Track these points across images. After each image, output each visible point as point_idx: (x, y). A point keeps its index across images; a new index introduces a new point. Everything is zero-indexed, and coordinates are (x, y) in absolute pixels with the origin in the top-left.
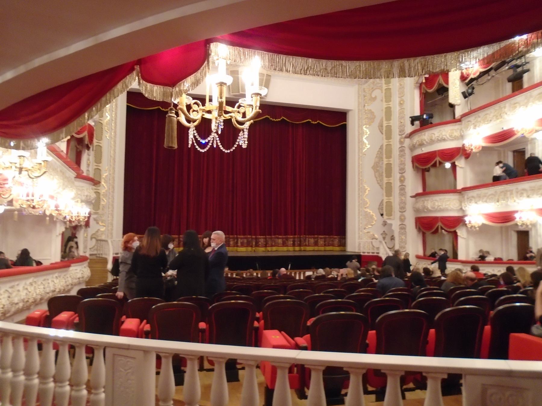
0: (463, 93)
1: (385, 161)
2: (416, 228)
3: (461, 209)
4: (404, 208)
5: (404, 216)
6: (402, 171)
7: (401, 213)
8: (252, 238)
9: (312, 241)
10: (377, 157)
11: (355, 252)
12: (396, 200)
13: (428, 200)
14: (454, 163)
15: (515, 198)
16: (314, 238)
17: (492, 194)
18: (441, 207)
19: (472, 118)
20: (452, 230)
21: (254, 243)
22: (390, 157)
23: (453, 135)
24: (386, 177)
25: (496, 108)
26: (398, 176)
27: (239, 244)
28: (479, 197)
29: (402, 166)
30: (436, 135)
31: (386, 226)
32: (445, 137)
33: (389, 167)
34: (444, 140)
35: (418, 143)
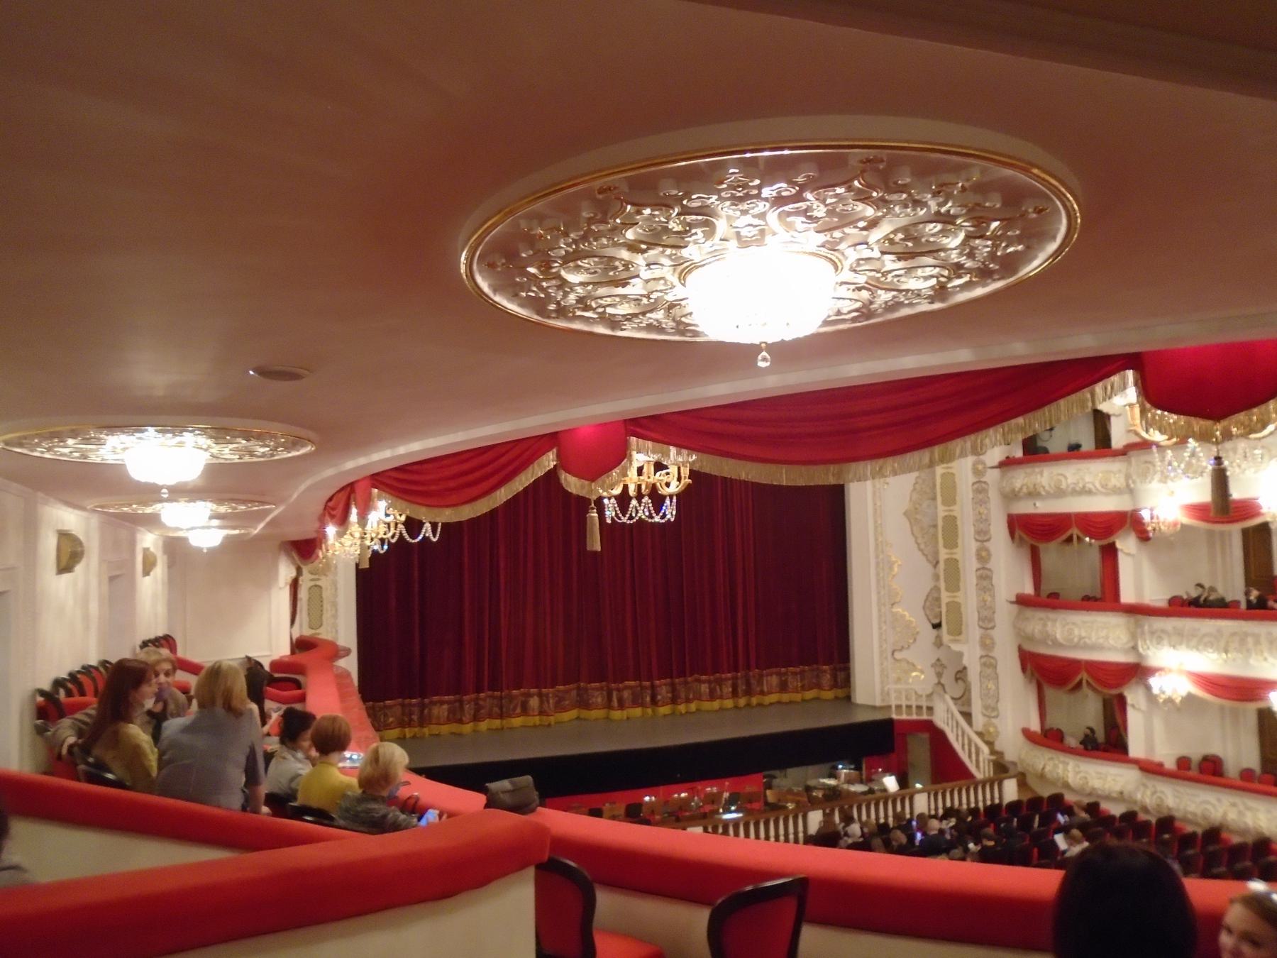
2: (1024, 669)
3: (1135, 648)
4: (991, 620)
5: (992, 639)
6: (983, 535)
8: (642, 688)
10: (914, 489)
11: (874, 708)
12: (969, 598)
13: (1055, 621)
15: (1266, 654)
16: (779, 674)
20: (1115, 692)
21: (648, 699)
22: (953, 502)
24: (945, 547)
26: (974, 546)
27: (615, 703)
30: (1070, 481)
32: (1090, 486)
33: (951, 522)
34: (1090, 492)
35: (1025, 490)
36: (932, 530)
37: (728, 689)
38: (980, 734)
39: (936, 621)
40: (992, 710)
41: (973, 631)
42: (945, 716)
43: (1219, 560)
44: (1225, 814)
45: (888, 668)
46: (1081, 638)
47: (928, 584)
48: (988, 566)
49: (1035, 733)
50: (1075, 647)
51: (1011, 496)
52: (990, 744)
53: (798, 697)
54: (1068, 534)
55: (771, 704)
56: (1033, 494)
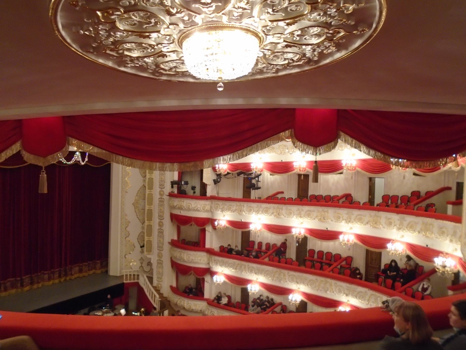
0: (214, 180)
3: (209, 263)
4: (162, 247)
5: (162, 254)
6: (161, 217)
9: (77, 269)
12: (155, 239)
14: (205, 228)
15: (247, 272)
19: (220, 203)
20: (201, 277)
21: (19, 285)
24: (147, 220)
26: (158, 221)
30: (193, 206)
33: (150, 212)
34: (199, 211)
36: (142, 211)
37: (57, 275)
39: (142, 245)
40: (160, 278)
42: (143, 282)
43: (235, 234)
45: (122, 260)
46: (192, 260)
47: (139, 230)
50: (191, 262)
51: (173, 207)
52: (158, 291)
53: (86, 274)
54: (191, 223)
55: (75, 278)
56: (180, 208)
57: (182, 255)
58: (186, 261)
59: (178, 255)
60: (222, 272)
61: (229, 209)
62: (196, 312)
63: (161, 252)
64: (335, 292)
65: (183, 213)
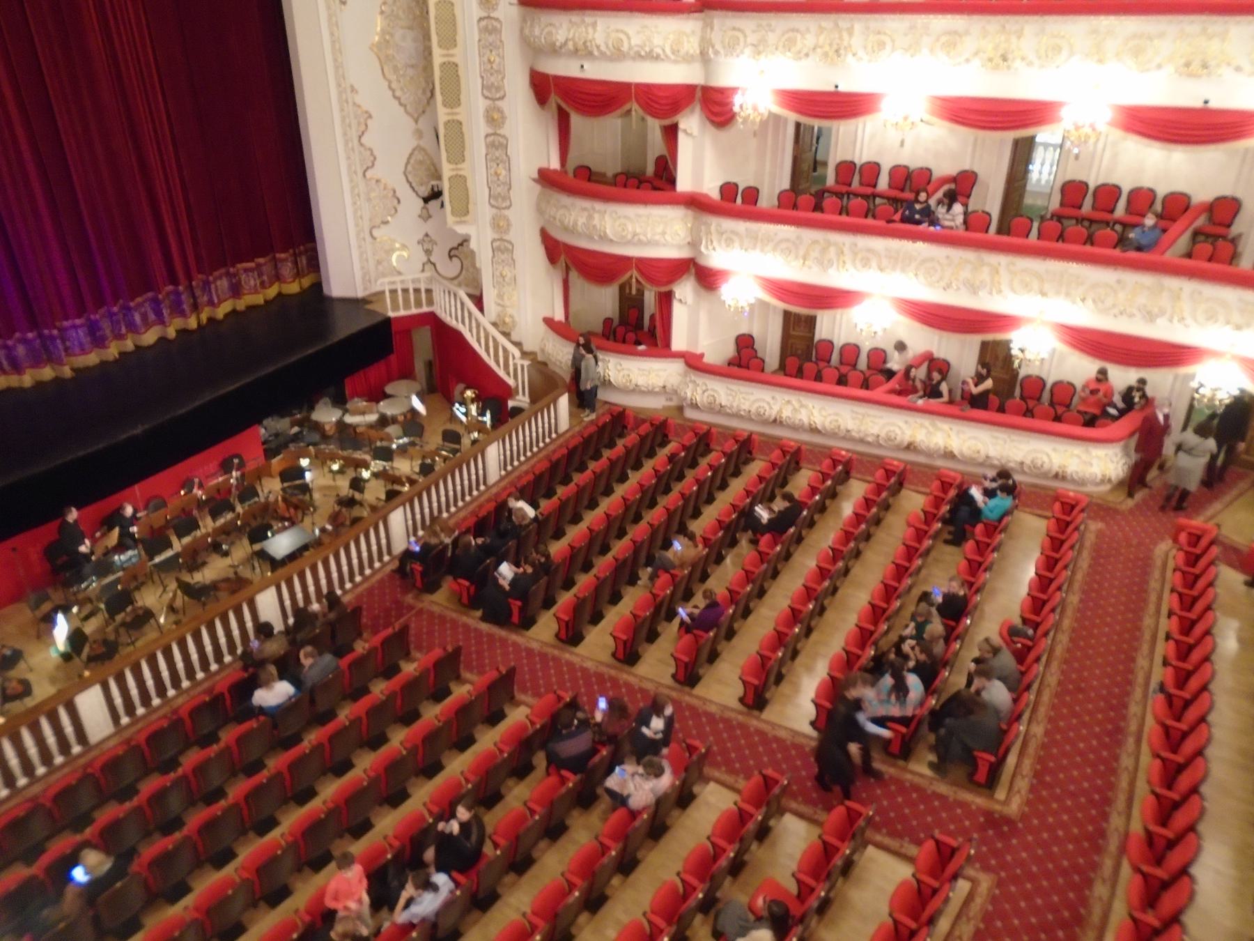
1: (438, 57)
6: (493, 91)
7: (494, 211)
16: (228, 274)
17: (787, 240)
18: (642, 237)
23: (682, 52)
25: (824, 24)
26: (481, 104)
28: (756, 238)
29: (492, 79)
31: (430, 221)
32: (659, 51)
34: (657, 58)
35: (570, 45)
38: (494, 324)
41: (482, 208)
42: (450, 310)
44: (780, 411)
45: (367, 247)
46: (635, 234)
47: (406, 142)
48: (501, 132)
49: (560, 322)
50: (629, 243)
54: (627, 107)
56: (583, 52)
57: (596, 221)
58: (611, 241)
59: (582, 221)
60: (753, 268)
61: (789, 45)
62: (650, 392)
63: (506, 212)
64: (1189, 321)
65: (595, 71)
